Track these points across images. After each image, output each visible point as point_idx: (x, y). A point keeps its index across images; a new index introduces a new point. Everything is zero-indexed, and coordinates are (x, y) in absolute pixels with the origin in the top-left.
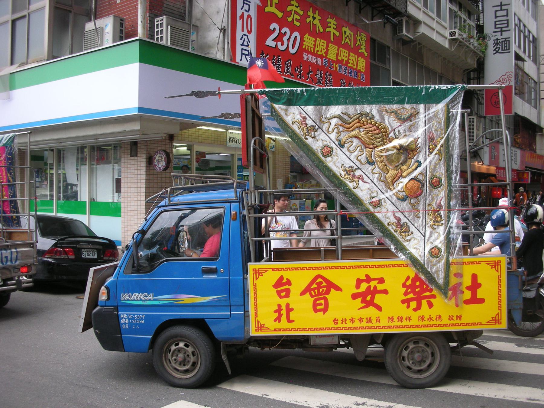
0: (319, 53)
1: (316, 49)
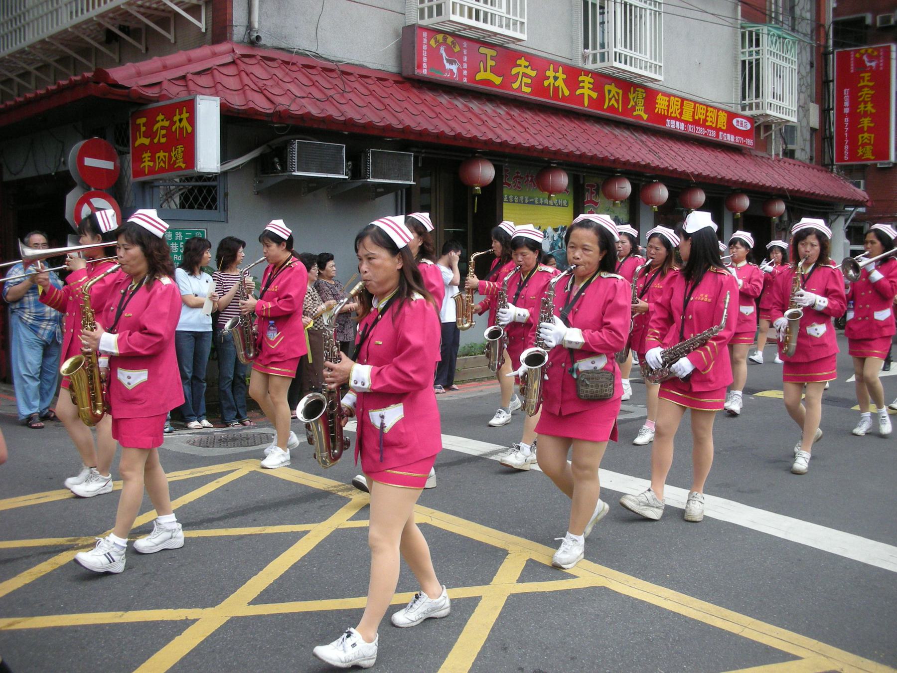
0: (673, 115)
1: (670, 111)
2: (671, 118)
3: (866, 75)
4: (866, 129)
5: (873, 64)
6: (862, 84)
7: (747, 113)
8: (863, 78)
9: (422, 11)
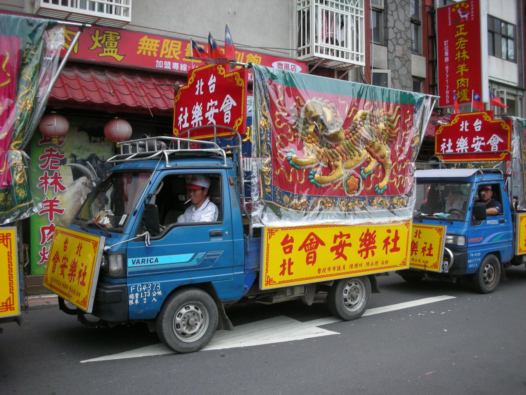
0: (169, 56)
1: (163, 52)
2: (164, 59)
4: (462, 74)
5: (466, 16)
6: (458, 35)
7: (302, 58)
8: (459, 29)
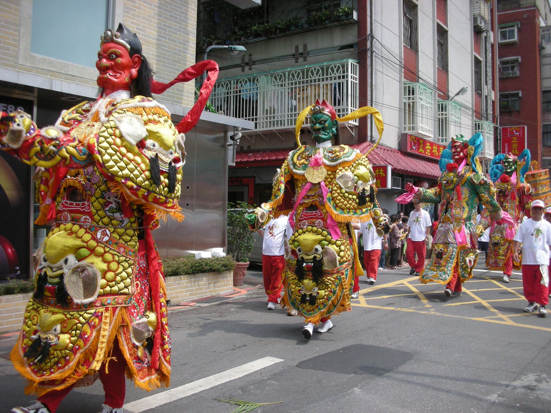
3: (515, 138)
5: (518, 134)
9: (405, 127)
